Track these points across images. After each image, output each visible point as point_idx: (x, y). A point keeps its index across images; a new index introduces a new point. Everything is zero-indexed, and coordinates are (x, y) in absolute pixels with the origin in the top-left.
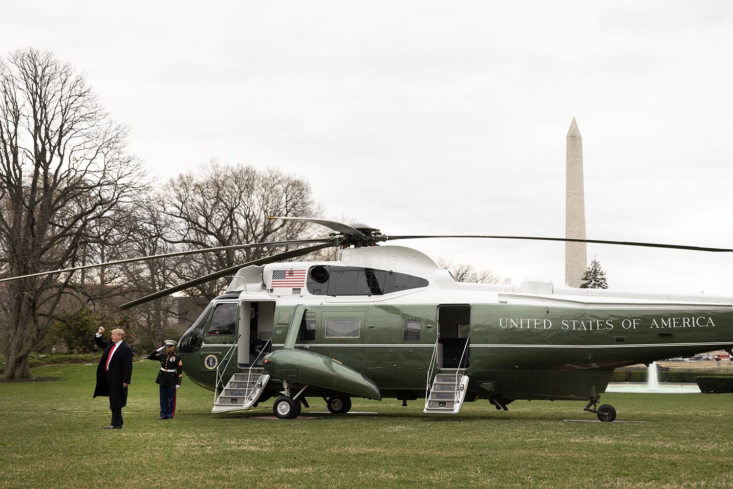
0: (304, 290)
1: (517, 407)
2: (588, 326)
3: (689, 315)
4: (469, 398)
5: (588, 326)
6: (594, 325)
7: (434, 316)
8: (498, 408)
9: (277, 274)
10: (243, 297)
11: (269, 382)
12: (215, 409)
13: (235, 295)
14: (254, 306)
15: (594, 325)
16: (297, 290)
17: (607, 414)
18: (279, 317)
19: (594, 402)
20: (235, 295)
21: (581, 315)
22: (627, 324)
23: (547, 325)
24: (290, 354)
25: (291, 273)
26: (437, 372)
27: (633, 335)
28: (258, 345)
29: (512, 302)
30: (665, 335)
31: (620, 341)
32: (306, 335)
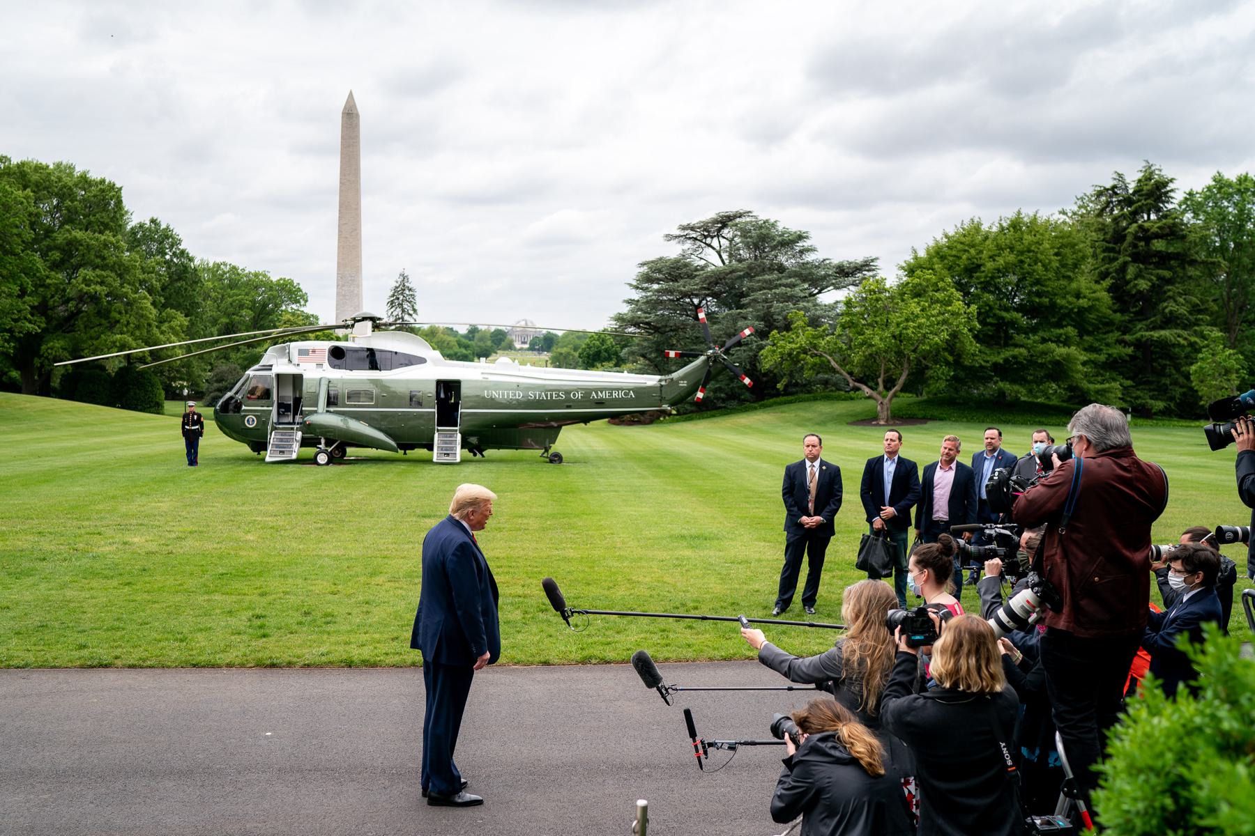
0: (326, 365)
7: (432, 389)
9: (302, 352)
10: (277, 369)
11: (303, 439)
12: (268, 459)
13: (269, 368)
16: (320, 365)
17: (557, 459)
18: (306, 388)
19: (547, 451)
20: (269, 368)
21: (547, 390)
23: (519, 395)
24: (323, 417)
25: (314, 351)
27: (578, 404)
28: (283, 408)
29: (492, 378)
30: (600, 403)
31: (569, 407)
32: (332, 401)
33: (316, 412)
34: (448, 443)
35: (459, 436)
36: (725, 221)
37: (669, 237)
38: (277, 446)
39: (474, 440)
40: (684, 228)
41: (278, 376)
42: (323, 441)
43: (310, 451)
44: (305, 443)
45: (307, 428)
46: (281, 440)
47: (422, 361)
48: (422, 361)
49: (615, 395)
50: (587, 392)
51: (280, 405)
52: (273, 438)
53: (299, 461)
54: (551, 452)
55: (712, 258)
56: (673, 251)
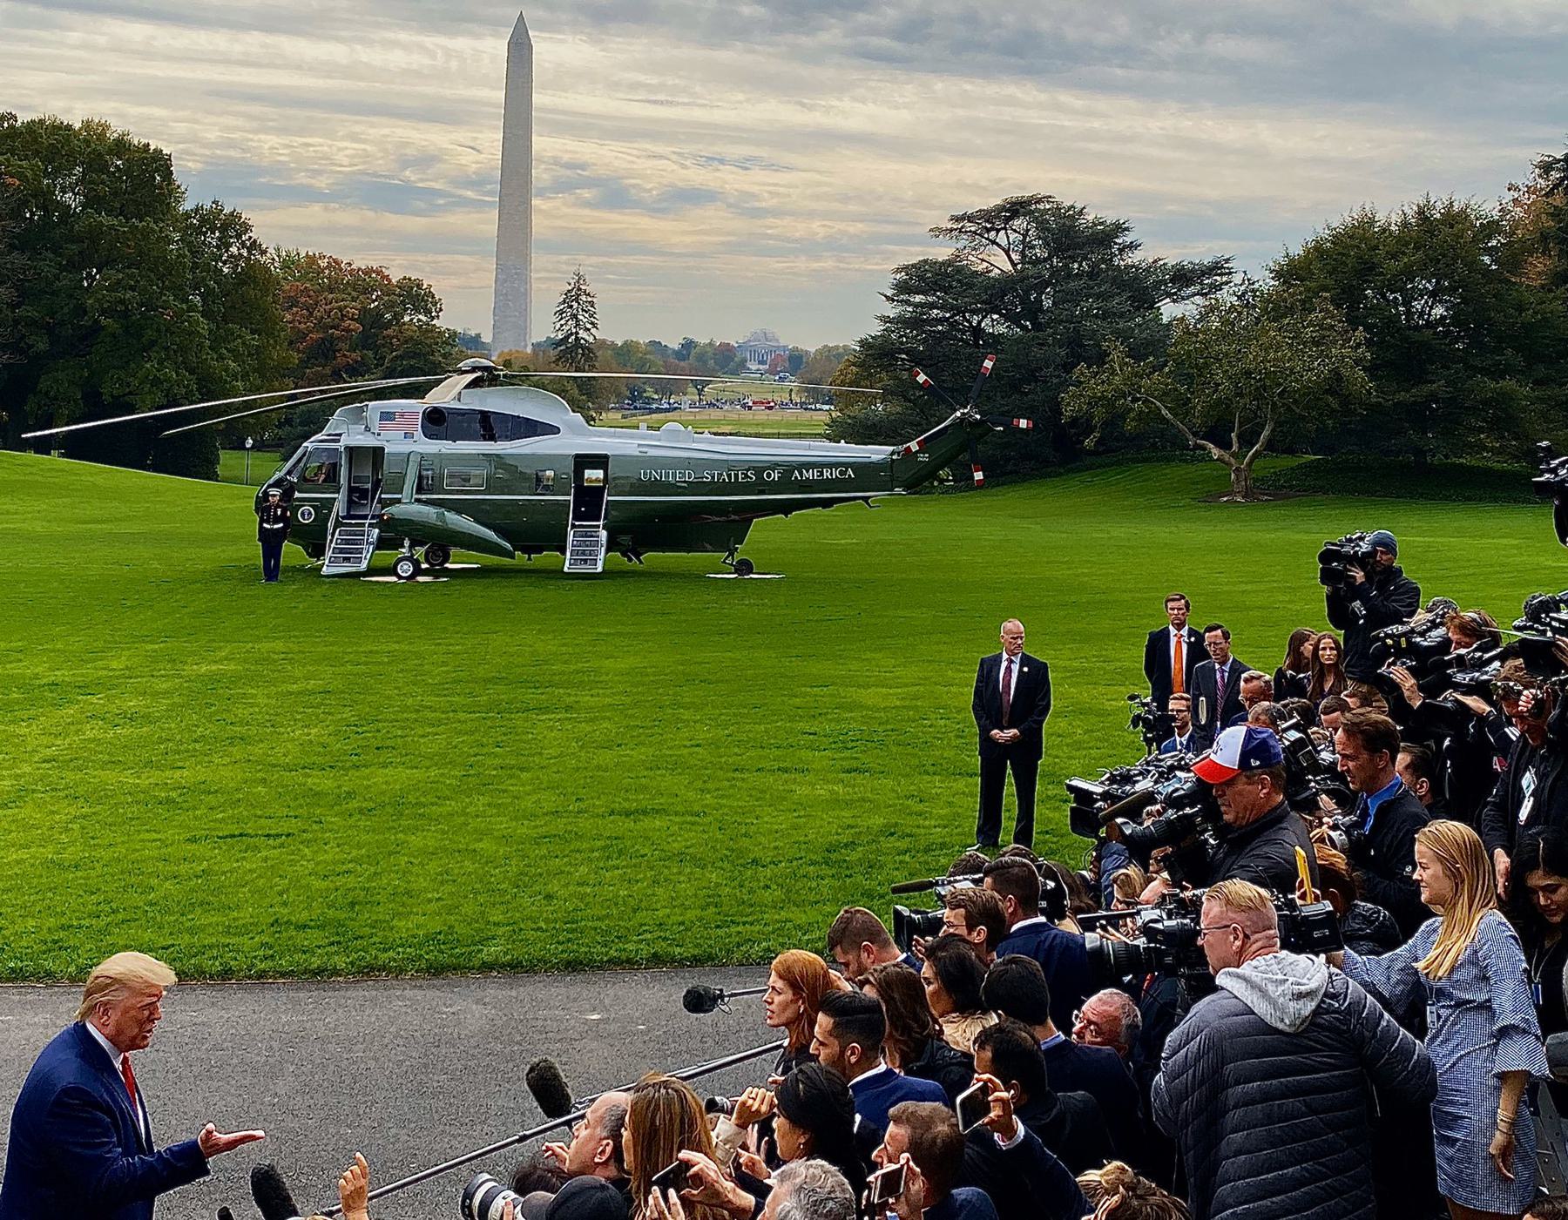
1: (652, 558)
2: (729, 476)
3: (830, 466)
4: (608, 551)
5: (729, 476)
6: (736, 476)
7: (570, 466)
8: (630, 560)
10: (345, 441)
11: (380, 538)
14: (351, 450)
15: (736, 476)
17: (744, 567)
19: (731, 554)
22: (769, 475)
24: (409, 508)
26: (574, 526)
28: (357, 496)
33: (399, 501)
34: (589, 548)
35: (604, 534)
36: (1016, 208)
37: (937, 231)
38: (341, 551)
39: (625, 539)
40: (957, 219)
41: (346, 448)
42: (407, 543)
43: (388, 557)
44: (381, 544)
45: (385, 524)
46: (347, 542)
47: (554, 430)
48: (554, 430)
49: (827, 474)
50: (788, 468)
51: (351, 490)
52: (334, 540)
53: (371, 571)
54: (737, 557)
55: (997, 261)
56: (942, 252)
